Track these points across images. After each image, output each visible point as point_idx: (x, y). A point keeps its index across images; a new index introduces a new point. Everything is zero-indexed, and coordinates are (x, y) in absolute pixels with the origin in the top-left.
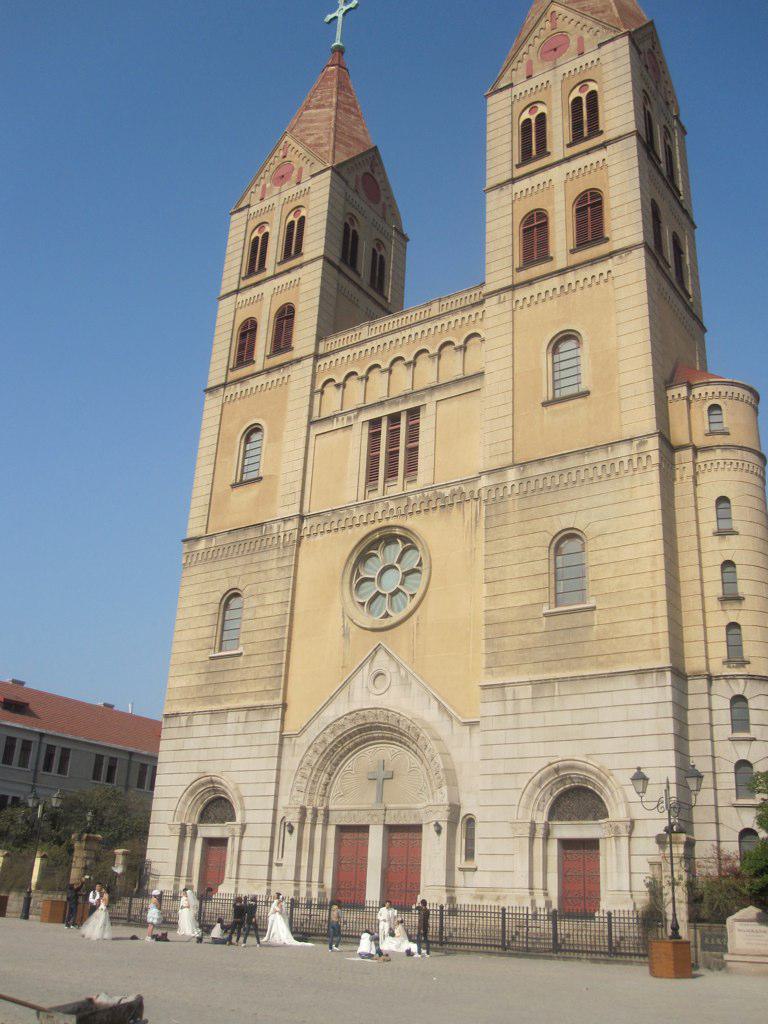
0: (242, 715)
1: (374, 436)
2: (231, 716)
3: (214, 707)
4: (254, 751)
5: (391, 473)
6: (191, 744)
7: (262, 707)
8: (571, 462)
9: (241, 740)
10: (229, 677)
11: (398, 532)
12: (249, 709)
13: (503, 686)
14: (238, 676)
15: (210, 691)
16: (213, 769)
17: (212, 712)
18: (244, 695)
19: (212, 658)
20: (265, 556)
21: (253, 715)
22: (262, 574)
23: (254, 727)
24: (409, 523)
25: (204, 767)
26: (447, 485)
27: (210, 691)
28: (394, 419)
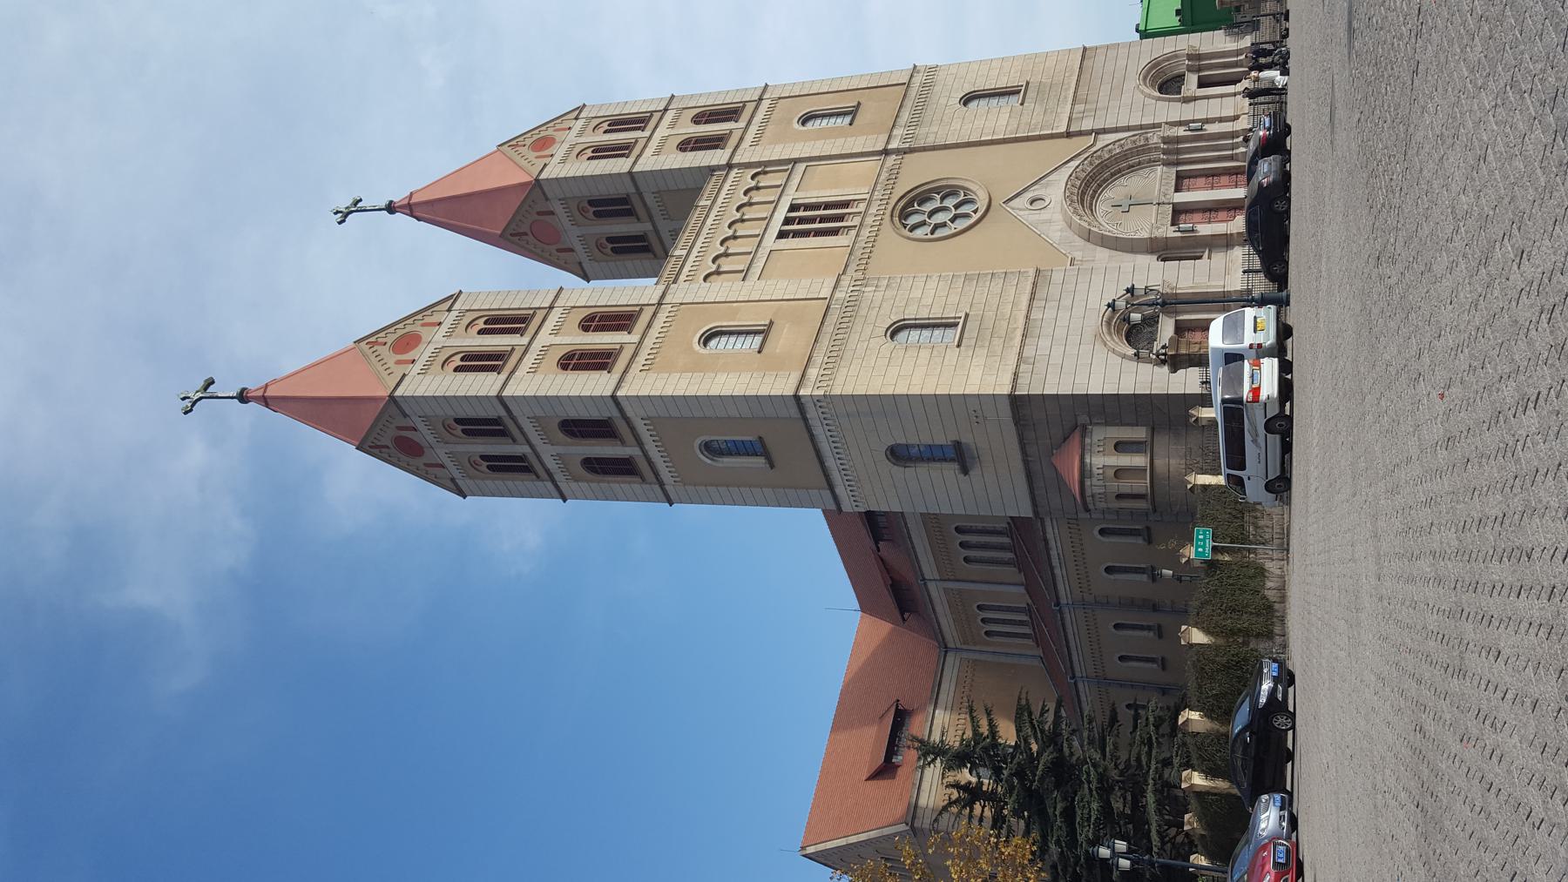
1: (797, 234)
3: (1019, 333)
4: (1082, 287)
5: (841, 218)
7: (1035, 284)
9: (1066, 302)
10: (989, 323)
12: (1032, 299)
13: (1070, 119)
14: (990, 314)
15: (997, 343)
17: (1024, 336)
20: (864, 305)
21: (1040, 294)
22: (884, 304)
23: (1055, 291)
24: (899, 192)
25: (1089, 336)
27: (997, 343)
28: (787, 221)
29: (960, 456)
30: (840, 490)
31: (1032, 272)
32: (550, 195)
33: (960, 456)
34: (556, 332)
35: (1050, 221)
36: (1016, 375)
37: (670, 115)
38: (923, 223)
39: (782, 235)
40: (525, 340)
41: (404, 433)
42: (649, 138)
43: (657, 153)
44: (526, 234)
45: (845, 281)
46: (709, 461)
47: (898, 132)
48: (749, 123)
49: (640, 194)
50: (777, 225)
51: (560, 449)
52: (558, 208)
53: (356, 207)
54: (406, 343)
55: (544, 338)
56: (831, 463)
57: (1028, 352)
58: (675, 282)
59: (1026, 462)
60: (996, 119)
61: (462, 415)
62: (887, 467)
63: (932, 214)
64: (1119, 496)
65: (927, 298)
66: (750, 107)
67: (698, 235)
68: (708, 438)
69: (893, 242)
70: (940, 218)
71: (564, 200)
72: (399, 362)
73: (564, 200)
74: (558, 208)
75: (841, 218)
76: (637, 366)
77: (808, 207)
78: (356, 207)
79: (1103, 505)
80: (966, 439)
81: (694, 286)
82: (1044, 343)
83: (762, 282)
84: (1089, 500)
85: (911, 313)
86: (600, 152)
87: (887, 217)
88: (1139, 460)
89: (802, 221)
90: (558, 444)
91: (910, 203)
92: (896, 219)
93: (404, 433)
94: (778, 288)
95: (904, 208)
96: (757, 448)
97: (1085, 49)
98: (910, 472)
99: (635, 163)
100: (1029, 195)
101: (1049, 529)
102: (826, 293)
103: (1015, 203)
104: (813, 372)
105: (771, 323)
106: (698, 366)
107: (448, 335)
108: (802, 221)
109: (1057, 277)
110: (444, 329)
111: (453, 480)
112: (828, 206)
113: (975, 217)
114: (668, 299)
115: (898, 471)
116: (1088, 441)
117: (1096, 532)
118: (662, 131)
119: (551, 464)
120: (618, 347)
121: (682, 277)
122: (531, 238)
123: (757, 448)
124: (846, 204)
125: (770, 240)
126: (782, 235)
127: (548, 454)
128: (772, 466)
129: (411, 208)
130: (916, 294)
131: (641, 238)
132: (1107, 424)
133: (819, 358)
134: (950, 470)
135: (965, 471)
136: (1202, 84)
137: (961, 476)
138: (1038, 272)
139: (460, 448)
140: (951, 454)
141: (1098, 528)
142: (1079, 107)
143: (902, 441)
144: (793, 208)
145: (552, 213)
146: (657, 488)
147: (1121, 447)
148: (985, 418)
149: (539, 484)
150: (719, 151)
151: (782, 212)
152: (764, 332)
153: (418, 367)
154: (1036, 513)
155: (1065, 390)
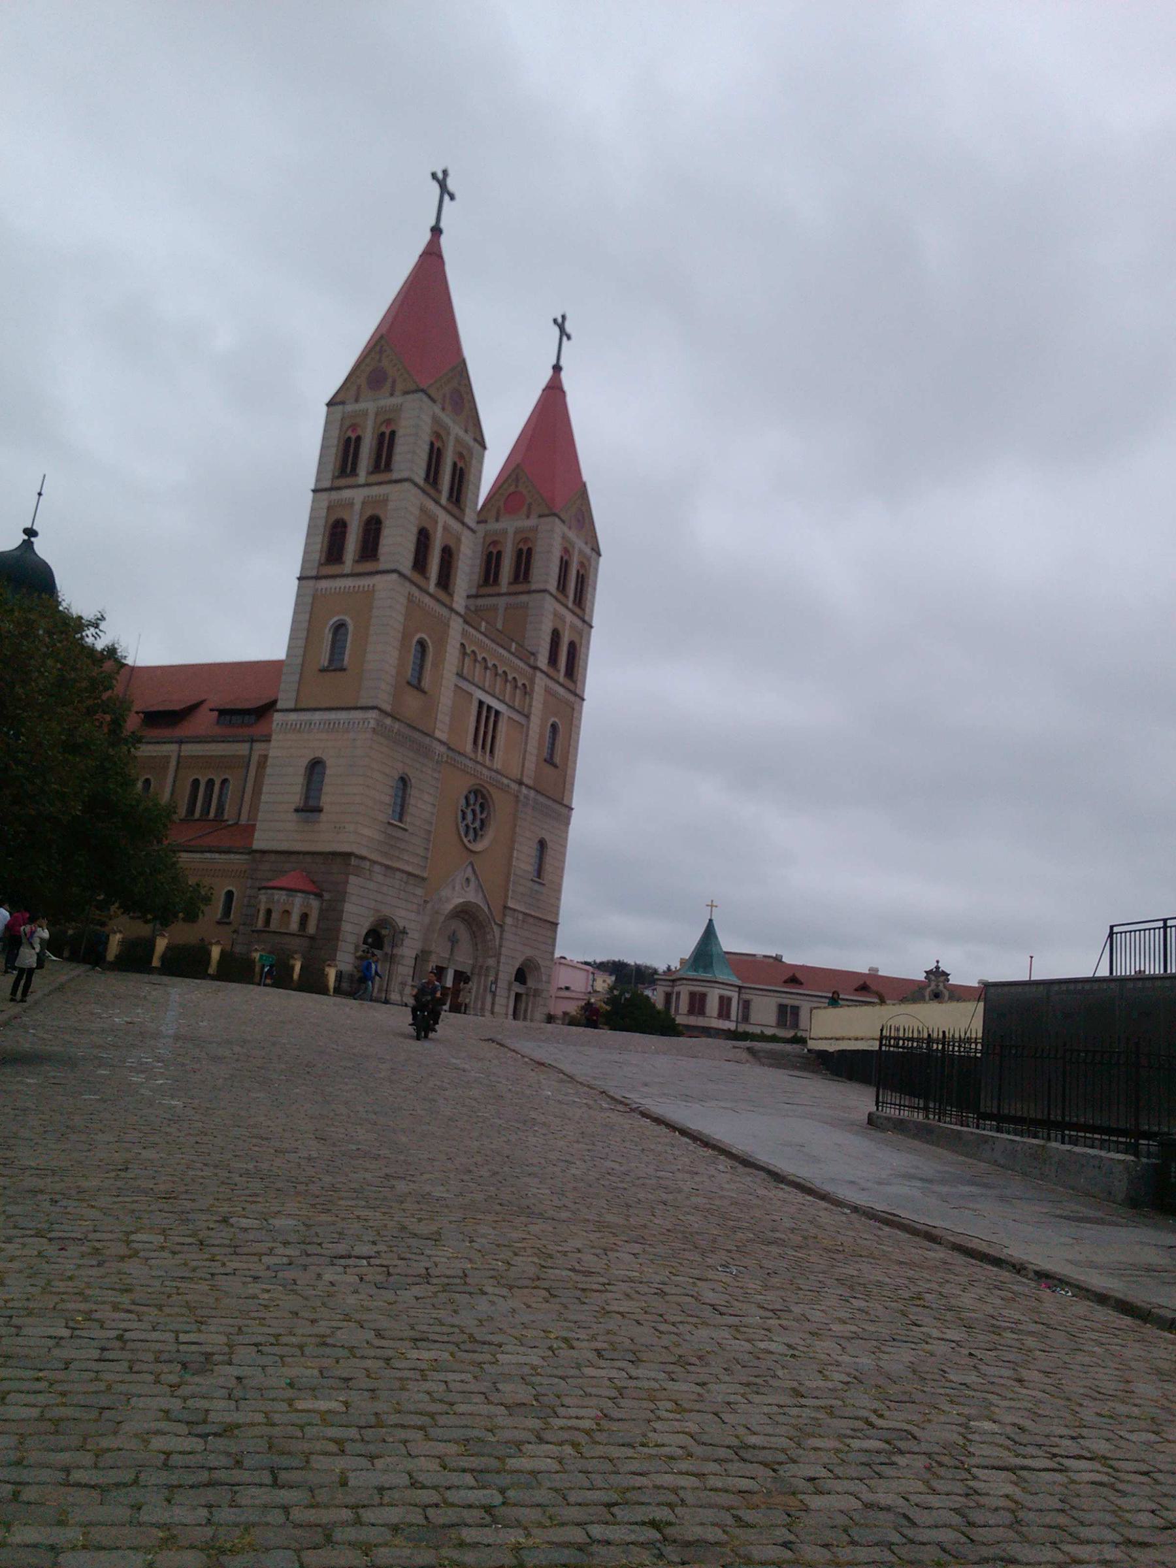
0: (405, 876)
2: (398, 875)
5: (483, 747)
6: (371, 885)
7: (416, 876)
8: (550, 803)
11: (485, 792)
12: (409, 874)
13: (515, 910)
16: (386, 911)
17: (387, 867)
18: (407, 862)
19: (389, 823)
24: (492, 790)
26: (507, 777)
28: (489, 708)
29: (310, 808)
30: (293, 716)
31: (425, 875)
32: (543, 520)
33: (310, 808)
34: (446, 528)
35: (454, 888)
36: (363, 858)
37: (579, 623)
38: (468, 804)
39: (481, 703)
40: (444, 501)
41: (390, 380)
42: (567, 607)
43: (556, 614)
44: (517, 486)
45: (443, 749)
46: (331, 622)
47: (532, 794)
48: (562, 685)
49: (529, 592)
50: (489, 700)
51: (358, 507)
52: (532, 522)
53: (563, 333)
56: (317, 716)
57: (377, 868)
58: (466, 622)
59: (298, 853)
60: (524, 862)
61: (399, 441)
62: (309, 755)
63: (473, 811)
64: (269, 912)
65: (422, 804)
66: (571, 686)
67: (493, 640)
68: (351, 628)
69: (461, 785)
70: (470, 817)
71: (535, 529)
72: (444, 396)
73: (535, 529)
74: (532, 522)
75: (483, 747)
77: (496, 723)
78: (563, 333)
79: (263, 898)
80: (323, 817)
81: (459, 637)
82: (380, 878)
83: (452, 688)
84: (269, 891)
85: (413, 792)
86: (564, 566)
87: (478, 782)
88: (294, 926)
89: (487, 718)
90: (362, 508)
91: (483, 797)
92: (476, 787)
93: (388, 384)
94: (446, 699)
95: (481, 792)
96: (335, 666)
97: (557, 924)
98: (302, 771)
99: (551, 594)
100: (473, 879)
101: (238, 857)
102: (438, 734)
103: (469, 869)
104: (388, 721)
105: (424, 692)
106: (406, 636)
107: (458, 441)
108: (487, 718)
109: (419, 891)
110: (461, 433)
111: (343, 403)
112: (493, 738)
113: (465, 840)
114: (454, 616)
115: (304, 762)
116: (312, 897)
117: (230, 888)
118: (569, 617)
119: (347, 494)
120: (428, 575)
121: (466, 627)
122: (512, 489)
123: (335, 666)
124: (492, 751)
125: (479, 694)
126: (481, 703)
128: (321, 671)
130: (426, 797)
131: (496, 581)
132: (321, 910)
135: (297, 810)
136: (518, 996)
137: (293, 806)
138: (424, 879)
139: (370, 424)
140: (312, 803)
141: (234, 890)
142: (521, 917)
143: (328, 772)
144: (497, 713)
145: (528, 517)
146: (314, 573)
147: (304, 918)
148: (338, 833)
149: (330, 476)
150: (547, 662)
151: (496, 704)
152: (418, 688)
154: (253, 852)
155: (351, 889)
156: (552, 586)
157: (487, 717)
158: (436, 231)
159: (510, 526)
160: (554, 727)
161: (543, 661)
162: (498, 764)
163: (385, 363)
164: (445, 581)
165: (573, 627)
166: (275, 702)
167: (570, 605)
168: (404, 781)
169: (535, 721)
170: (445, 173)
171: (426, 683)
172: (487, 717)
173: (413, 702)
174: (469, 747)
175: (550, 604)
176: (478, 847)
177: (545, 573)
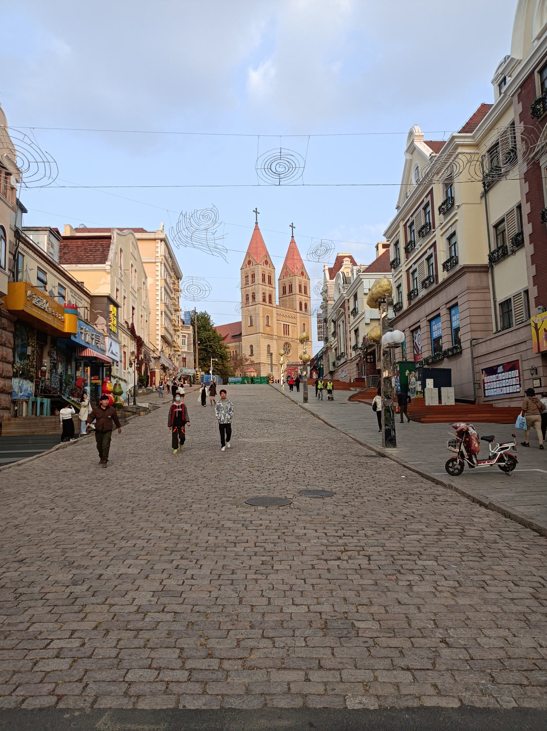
37: (307, 298)
52: (291, 278)
54: (266, 262)
55: (268, 288)
71: (292, 280)
73: (292, 280)
74: (291, 278)
76: (263, 306)
86: (300, 286)
94: (275, 326)
96: (251, 325)
119: (247, 288)
123: (251, 325)
127: (250, 288)
129: (293, 242)
133: (265, 335)
134: (250, 354)
151: (287, 324)
153: (262, 266)
156: (298, 292)
157: (286, 327)
158: (257, 223)
159: (287, 280)
160: (304, 324)
161: (298, 310)
162: (290, 336)
163: (250, 259)
164: (270, 302)
165: (305, 300)
166: (241, 334)
167: (303, 294)
168: (269, 346)
169: (298, 324)
170: (256, 209)
171: (270, 325)
172: (286, 327)
173: (268, 329)
174: (282, 335)
175: (298, 296)
176: (288, 355)
177: (296, 289)
